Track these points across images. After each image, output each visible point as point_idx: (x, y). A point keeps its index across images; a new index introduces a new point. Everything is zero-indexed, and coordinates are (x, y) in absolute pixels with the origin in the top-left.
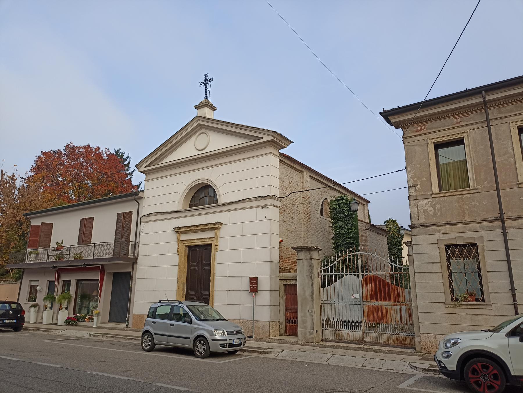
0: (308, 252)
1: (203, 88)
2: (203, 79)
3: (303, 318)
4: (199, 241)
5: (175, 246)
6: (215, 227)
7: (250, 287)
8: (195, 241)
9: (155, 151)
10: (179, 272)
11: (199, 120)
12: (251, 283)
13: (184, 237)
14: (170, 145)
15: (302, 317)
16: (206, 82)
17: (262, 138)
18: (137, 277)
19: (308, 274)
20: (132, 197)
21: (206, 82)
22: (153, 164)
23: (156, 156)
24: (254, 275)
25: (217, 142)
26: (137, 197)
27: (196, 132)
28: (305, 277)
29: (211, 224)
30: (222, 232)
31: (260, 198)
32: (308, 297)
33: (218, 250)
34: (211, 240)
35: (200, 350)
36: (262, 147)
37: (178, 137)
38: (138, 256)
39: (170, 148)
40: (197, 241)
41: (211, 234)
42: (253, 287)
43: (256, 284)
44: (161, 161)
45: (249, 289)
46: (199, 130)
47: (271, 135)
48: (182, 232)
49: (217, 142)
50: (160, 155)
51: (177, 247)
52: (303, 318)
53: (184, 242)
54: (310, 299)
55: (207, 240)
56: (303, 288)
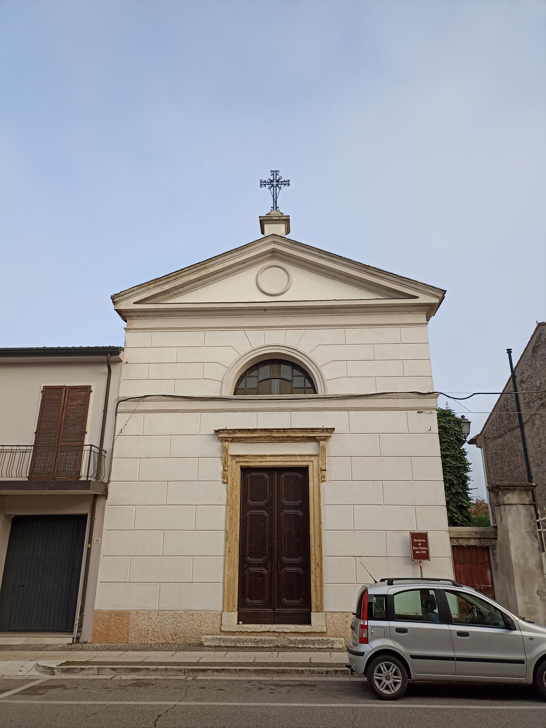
0: (524, 493)
1: (267, 191)
2: (268, 177)
3: (529, 606)
4: (280, 459)
5: (216, 467)
6: (318, 436)
7: (414, 551)
8: (268, 459)
9: (167, 276)
10: (230, 519)
11: (274, 242)
12: (414, 544)
13: (235, 449)
14: (204, 273)
15: (526, 603)
16: (275, 183)
17: (418, 297)
18: (106, 526)
19: (529, 530)
20: (104, 358)
21: (275, 183)
22: (150, 301)
23: (167, 287)
24: (421, 529)
25: (307, 288)
26: (113, 358)
27: (262, 261)
28: (525, 534)
29: (313, 430)
30: (333, 446)
31: (417, 395)
32: (534, 568)
33: (327, 478)
34: (307, 459)
35: (388, 683)
36: (409, 312)
37: (218, 264)
38: (109, 481)
39: (198, 279)
40: (272, 459)
41: (309, 448)
42: (421, 550)
43: (426, 544)
44: (171, 297)
45: (410, 554)
46: (267, 259)
47: (433, 295)
48: (234, 440)
49: (307, 288)
50: (176, 288)
51: (221, 468)
52: (529, 606)
53: (238, 459)
54: (538, 572)
55: (299, 459)
56: (523, 554)
